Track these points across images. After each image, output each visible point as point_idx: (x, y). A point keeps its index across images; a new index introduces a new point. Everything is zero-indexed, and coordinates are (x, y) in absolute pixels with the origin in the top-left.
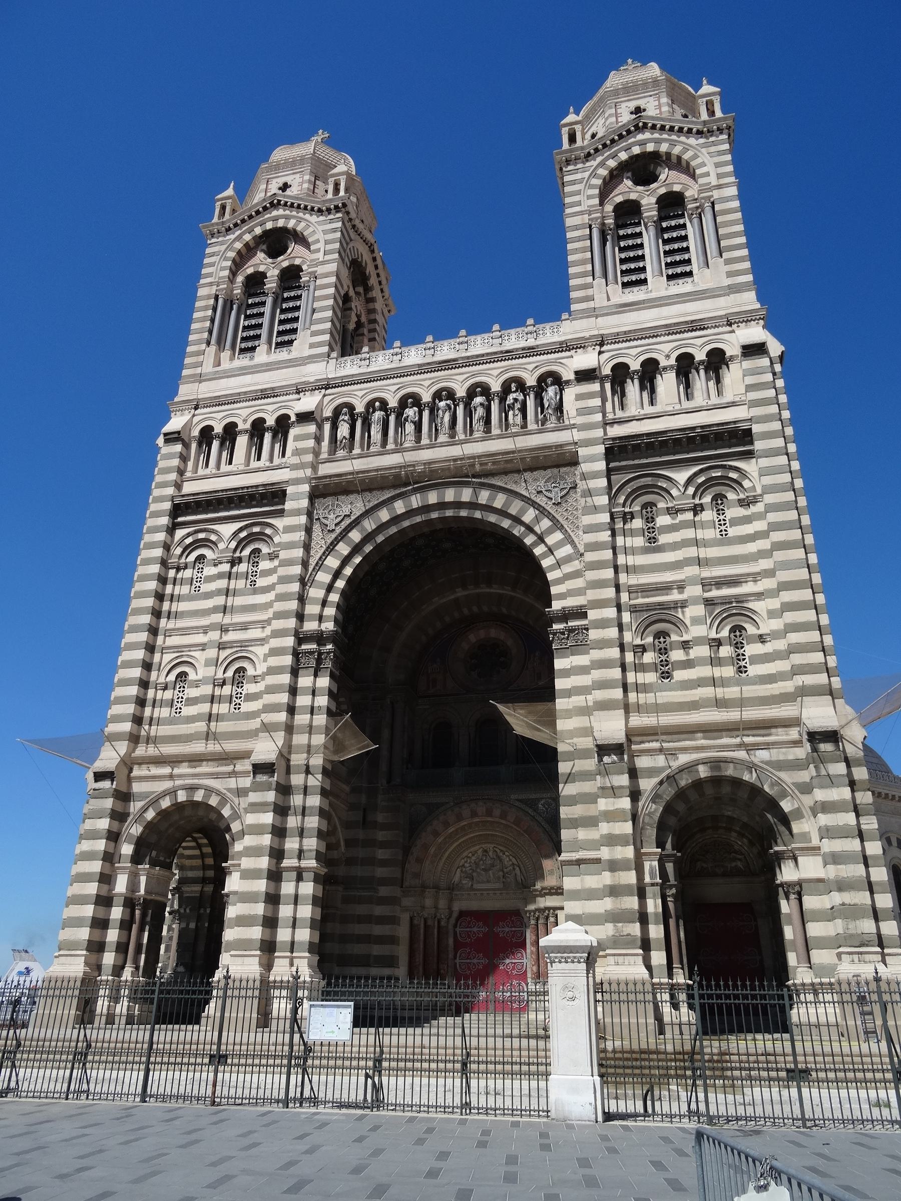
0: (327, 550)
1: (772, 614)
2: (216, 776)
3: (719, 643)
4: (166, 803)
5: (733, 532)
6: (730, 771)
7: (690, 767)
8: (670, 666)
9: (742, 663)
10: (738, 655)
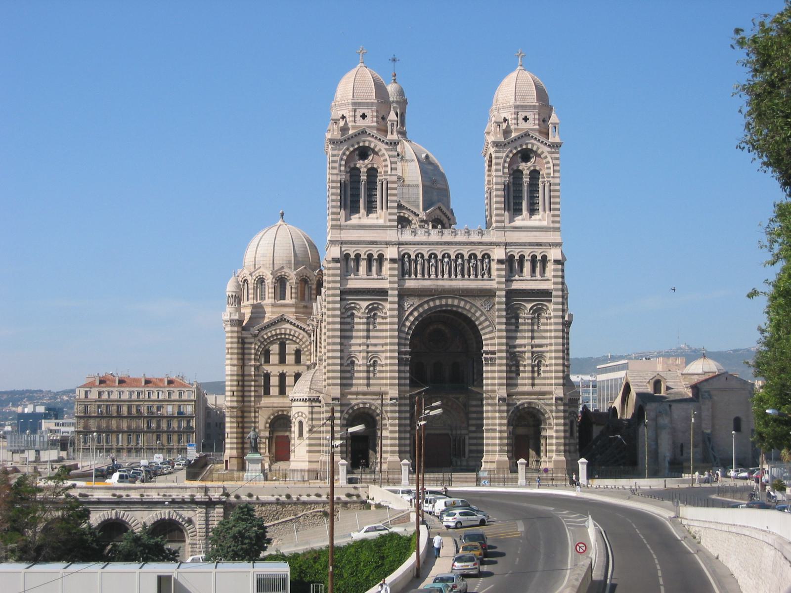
1: (551, 358)
2: (373, 400)
4: (356, 408)
6: (533, 406)
7: (523, 404)
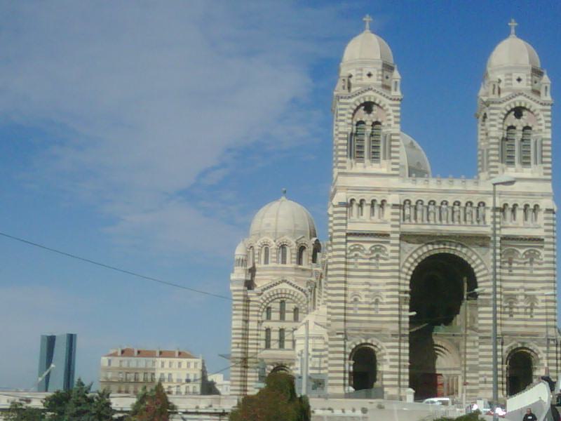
1: (543, 301)
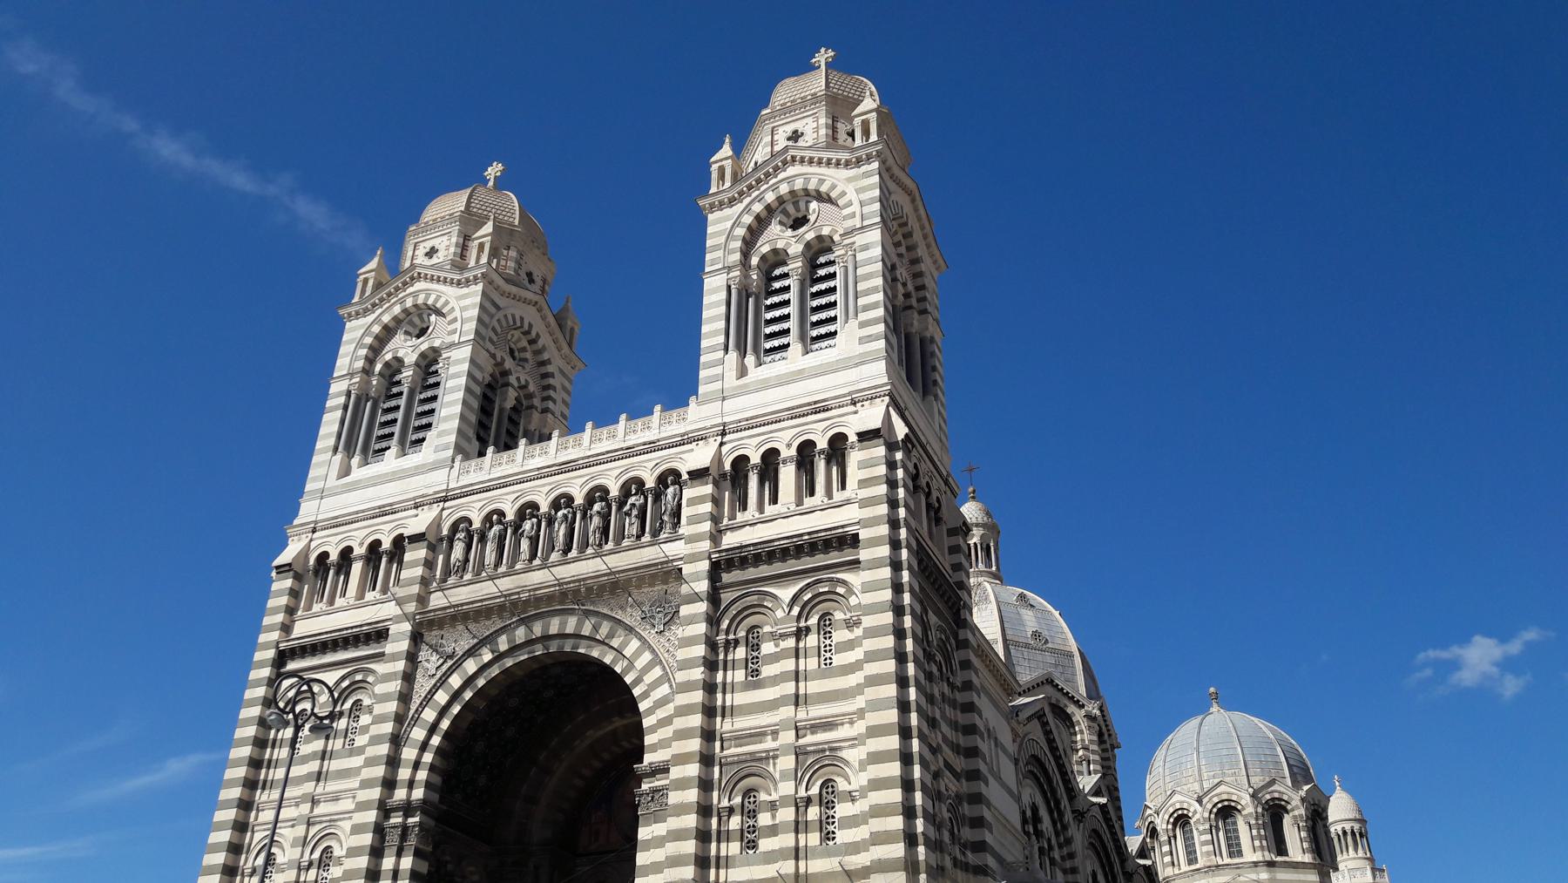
0: (424, 700)
1: (863, 765)
3: (809, 801)
5: (839, 660)
8: (757, 833)
9: (831, 828)
10: (828, 818)
